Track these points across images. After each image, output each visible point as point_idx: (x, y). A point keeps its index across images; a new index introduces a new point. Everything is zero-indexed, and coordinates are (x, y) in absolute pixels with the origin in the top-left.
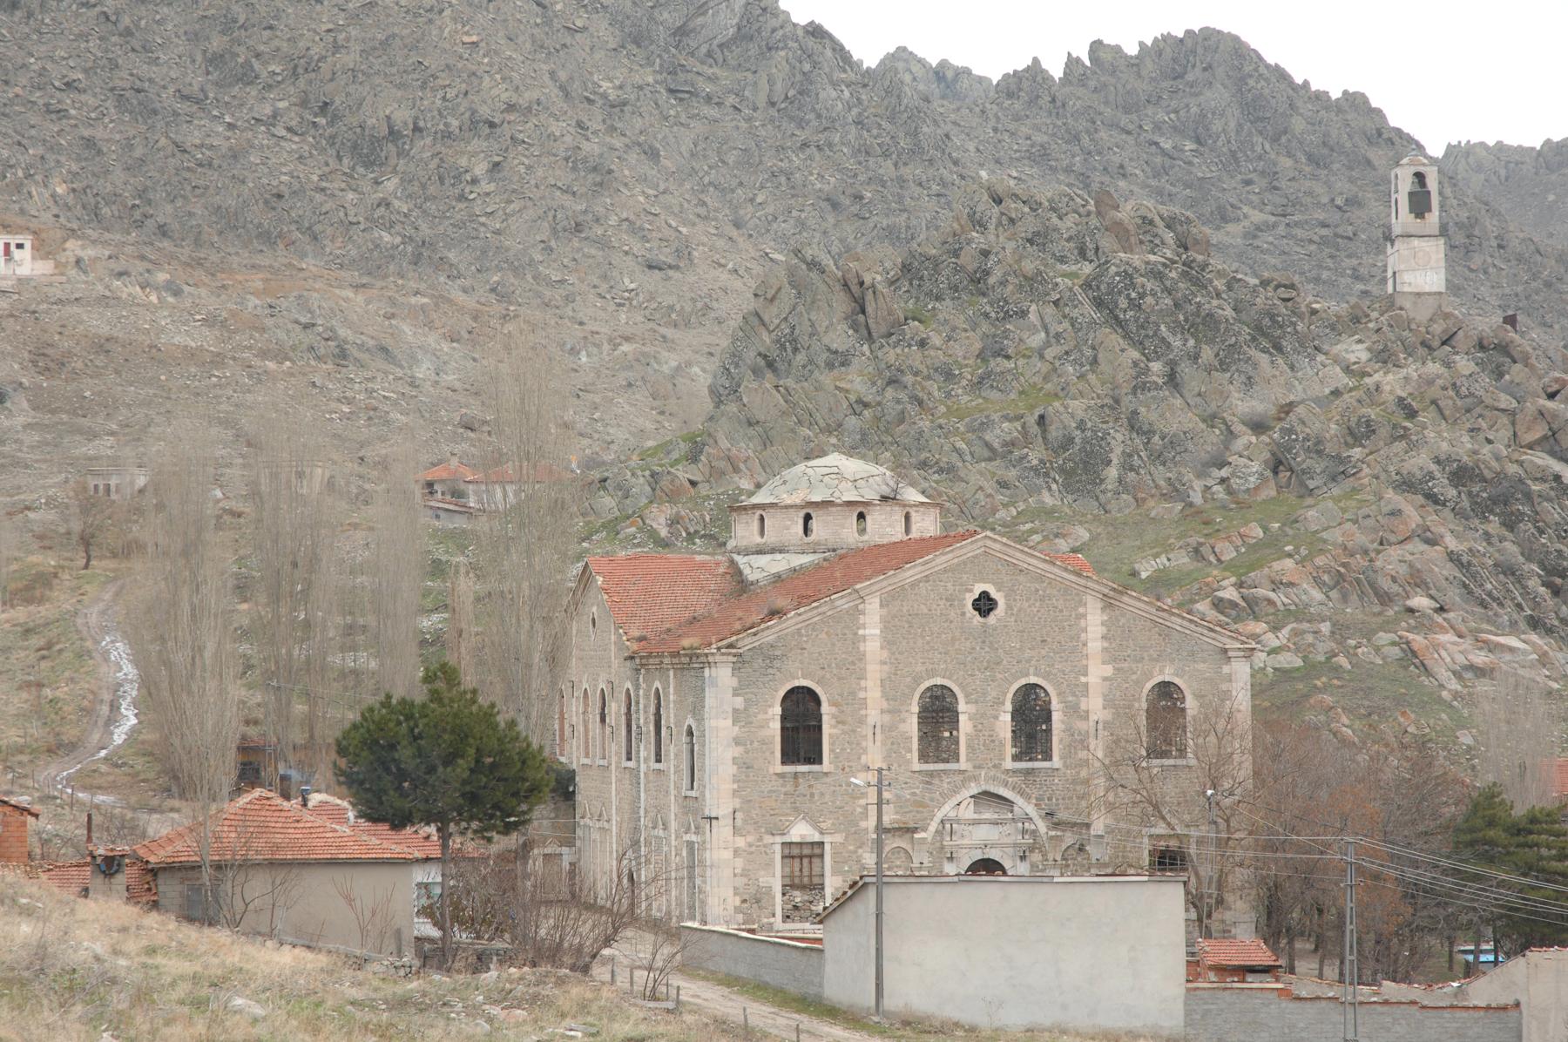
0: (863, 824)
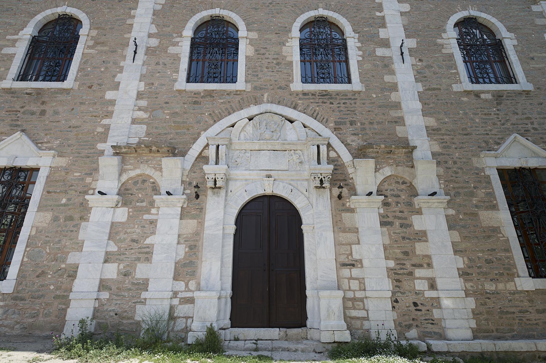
0: (100, 146)
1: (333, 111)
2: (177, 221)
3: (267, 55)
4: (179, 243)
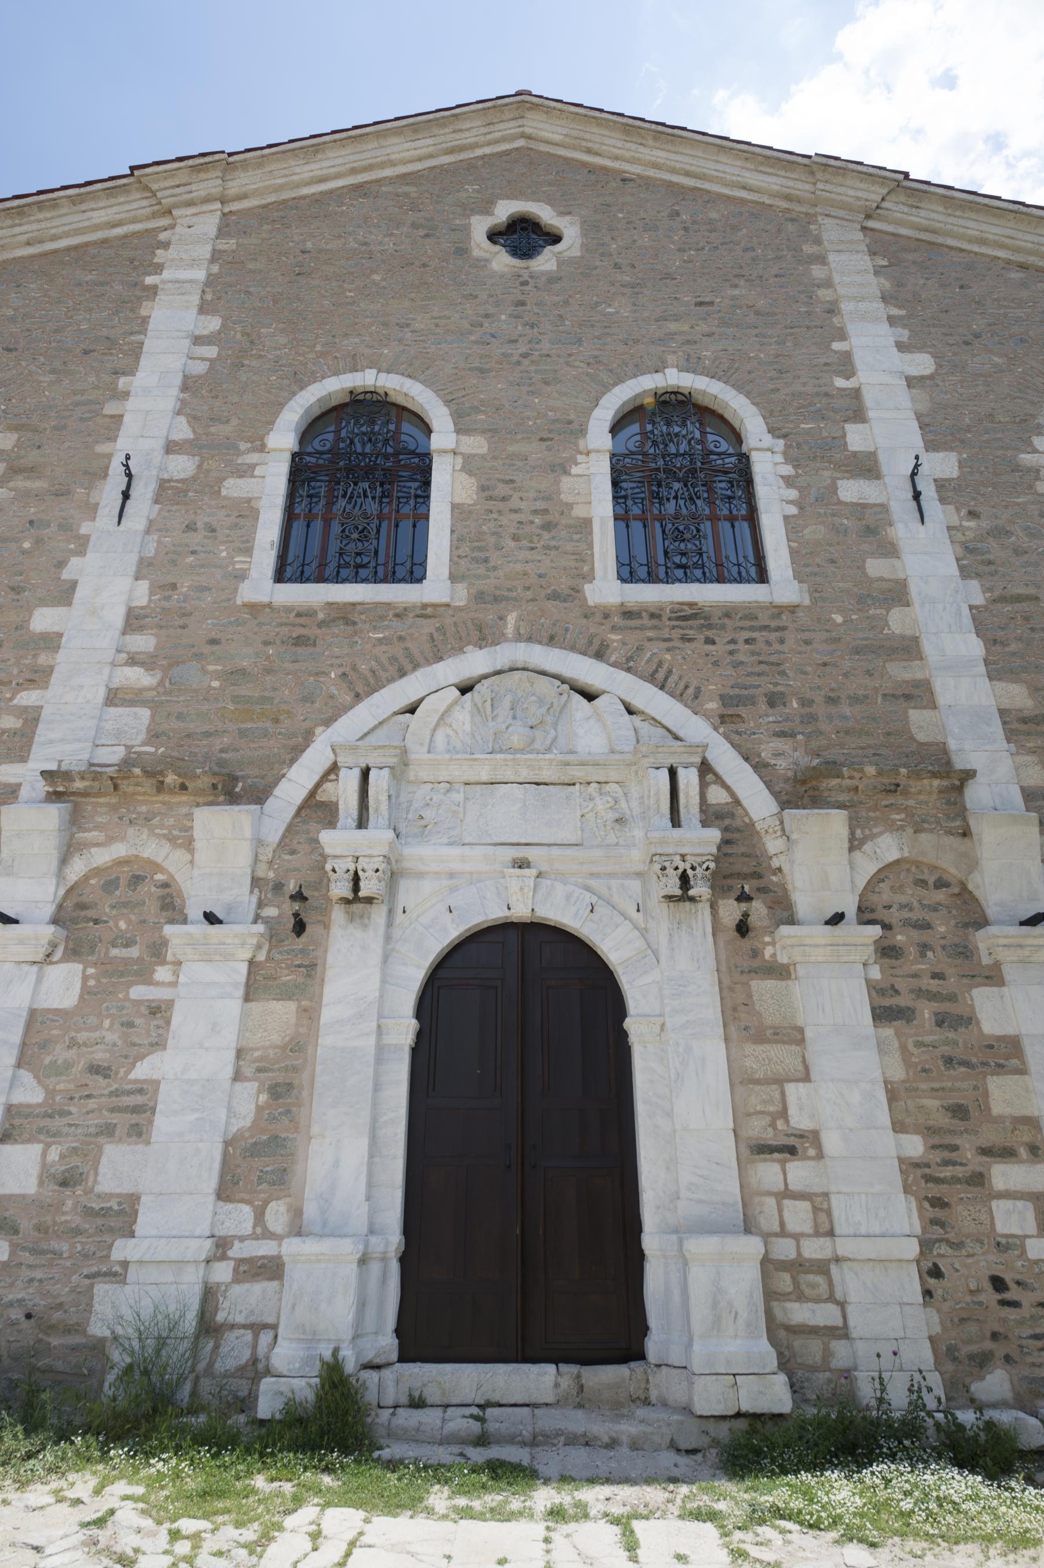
1: (716, 664)
2: (233, 1006)
3: (515, 503)
4: (237, 1077)
